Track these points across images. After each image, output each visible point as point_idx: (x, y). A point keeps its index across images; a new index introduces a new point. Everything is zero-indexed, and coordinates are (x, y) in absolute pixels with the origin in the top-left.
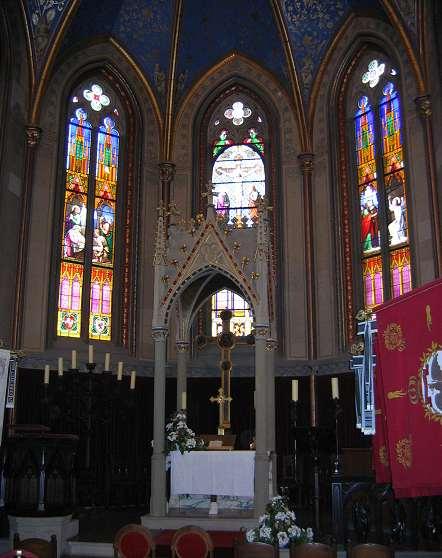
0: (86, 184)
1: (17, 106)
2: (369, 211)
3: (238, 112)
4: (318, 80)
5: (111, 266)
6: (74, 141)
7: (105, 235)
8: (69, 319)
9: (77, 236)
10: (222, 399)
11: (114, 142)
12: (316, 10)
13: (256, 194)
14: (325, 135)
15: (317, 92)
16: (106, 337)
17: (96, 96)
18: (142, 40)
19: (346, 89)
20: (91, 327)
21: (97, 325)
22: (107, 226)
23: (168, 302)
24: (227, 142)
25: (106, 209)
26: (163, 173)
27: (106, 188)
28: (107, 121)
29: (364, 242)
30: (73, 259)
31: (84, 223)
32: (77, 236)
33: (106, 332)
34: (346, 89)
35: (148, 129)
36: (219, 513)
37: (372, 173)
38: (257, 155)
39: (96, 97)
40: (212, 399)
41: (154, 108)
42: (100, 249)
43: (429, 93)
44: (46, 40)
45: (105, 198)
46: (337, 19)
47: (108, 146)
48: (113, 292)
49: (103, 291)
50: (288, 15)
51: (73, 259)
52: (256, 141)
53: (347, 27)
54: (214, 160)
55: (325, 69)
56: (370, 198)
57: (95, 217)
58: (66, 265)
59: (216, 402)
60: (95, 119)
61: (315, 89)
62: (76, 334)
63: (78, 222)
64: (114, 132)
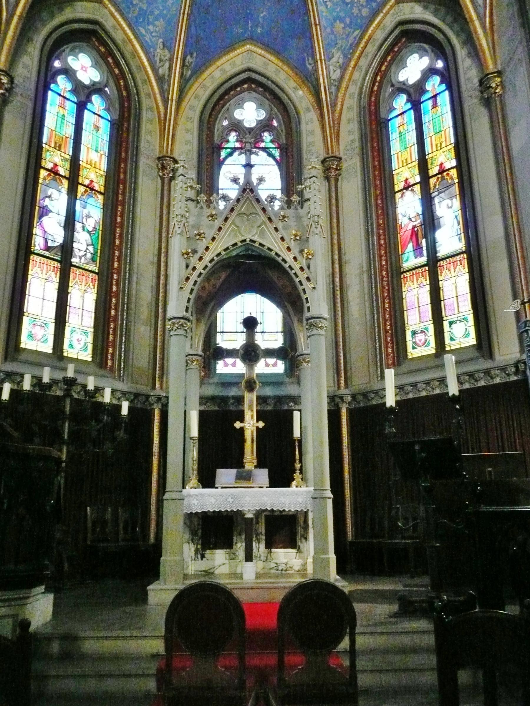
4: (347, 77)
7: (89, 232)
11: (105, 127)
14: (356, 136)
15: (346, 90)
17: (83, 67)
19: (380, 88)
24: (238, 145)
25: (91, 201)
26: (163, 168)
27: (93, 176)
28: (96, 99)
30: (47, 254)
31: (63, 213)
35: (145, 115)
38: (271, 161)
41: (154, 94)
42: (83, 247)
43: (499, 67)
49: (84, 299)
51: (47, 254)
53: (386, 15)
54: (221, 163)
58: (38, 259)
61: (344, 85)
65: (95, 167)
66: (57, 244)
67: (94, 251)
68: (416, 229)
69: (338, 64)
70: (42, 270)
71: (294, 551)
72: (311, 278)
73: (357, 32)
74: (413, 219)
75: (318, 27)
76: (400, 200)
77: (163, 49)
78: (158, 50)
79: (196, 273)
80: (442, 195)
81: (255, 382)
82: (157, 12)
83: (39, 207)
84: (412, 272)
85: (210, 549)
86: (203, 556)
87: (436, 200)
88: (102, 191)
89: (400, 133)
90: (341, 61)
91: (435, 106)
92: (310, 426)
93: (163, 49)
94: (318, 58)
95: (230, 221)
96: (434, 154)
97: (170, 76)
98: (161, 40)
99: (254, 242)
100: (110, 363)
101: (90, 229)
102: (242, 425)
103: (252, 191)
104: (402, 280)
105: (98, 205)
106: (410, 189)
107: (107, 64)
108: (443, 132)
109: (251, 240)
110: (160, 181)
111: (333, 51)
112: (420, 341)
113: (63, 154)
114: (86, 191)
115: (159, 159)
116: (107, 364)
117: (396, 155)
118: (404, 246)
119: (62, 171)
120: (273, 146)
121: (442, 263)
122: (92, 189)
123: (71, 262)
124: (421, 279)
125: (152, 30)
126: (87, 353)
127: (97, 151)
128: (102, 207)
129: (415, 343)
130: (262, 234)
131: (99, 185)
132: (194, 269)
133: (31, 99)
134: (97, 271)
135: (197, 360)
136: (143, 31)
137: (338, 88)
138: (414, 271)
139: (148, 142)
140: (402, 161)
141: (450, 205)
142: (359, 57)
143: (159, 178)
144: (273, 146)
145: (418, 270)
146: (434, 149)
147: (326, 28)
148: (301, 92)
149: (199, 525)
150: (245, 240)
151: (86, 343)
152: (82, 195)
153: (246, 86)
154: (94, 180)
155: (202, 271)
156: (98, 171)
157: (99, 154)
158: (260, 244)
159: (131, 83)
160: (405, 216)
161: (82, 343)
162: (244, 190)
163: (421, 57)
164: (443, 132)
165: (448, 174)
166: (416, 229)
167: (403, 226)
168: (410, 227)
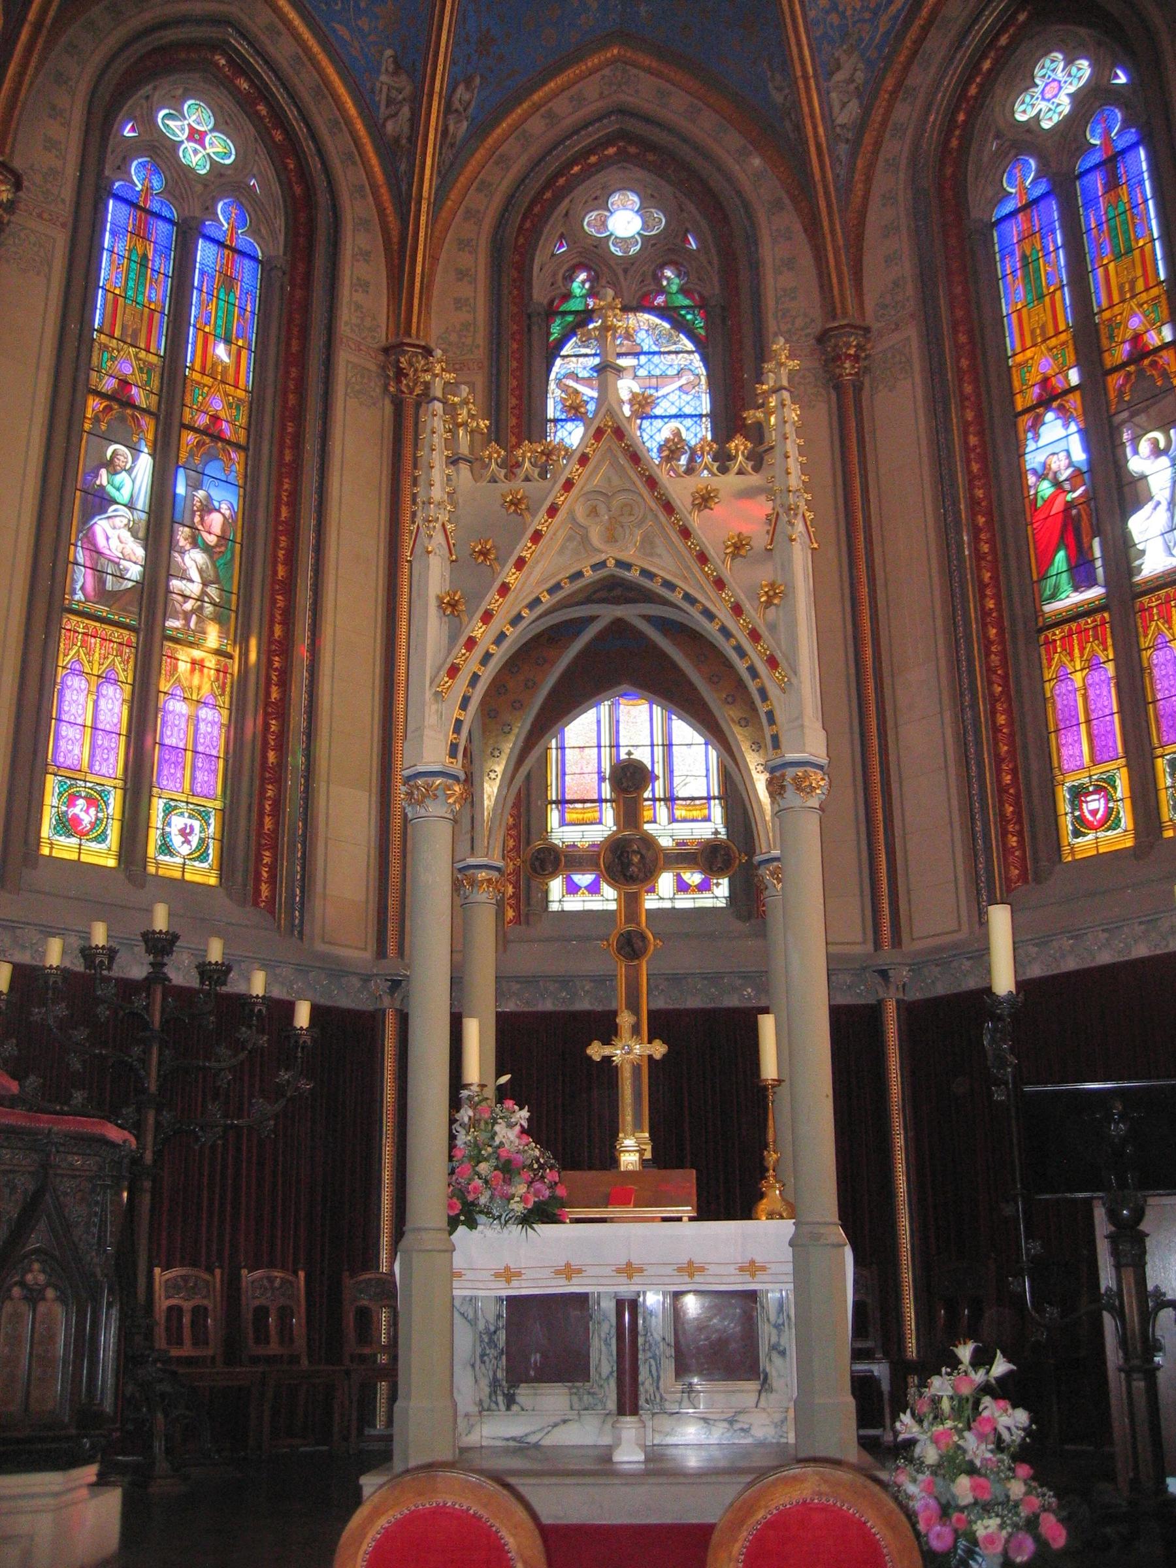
0: (155, 384)
2: (1057, 484)
3: (625, 221)
6: (120, 247)
7: (207, 549)
8: (81, 803)
9: (117, 538)
10: (631, 1051)
11: (248, 274)
14: (906, 268)
15: (876, 152)
16: (204, 873)
20: (154, 836)
21: (174, 830)
22: (216, 521)
23: (461, 684)
25: (213, 469)
27: (218, 406)
29: (1044, 577)
30: (102, 610)
31: (142, 502)
32: (117, 538)
33: (202, 857)
34: (964, 147)
36: (647, 1460)
37: (1063, 371)
39: (196, 136)
40: (596, 1051)
42: (194, 589)
47: (229, 281)
55: (899, 85)
56: (1055, 447)
57: (181, 490)
59: (607, 1059)
60: (191, 196)
61: (868, 139)
62: (103, 854)
63: (123, 496)
65: (223, 382)
66: (130, 584)
67: (220, 597)
68: (1074, 512)
69: (852, 87)
71: (753, 1386)
72: (779, 656)
74: (1067, 486)
77: (395, 73)
78: (383, 78)
79: (478, 652)
81: (643, 937)
84: (1066, 627)
86: (510, 1400)
89: (1024, 257)
90: (860, 76)
91: (1112, 185)
93: (395, 73)
94: (799, 74)
95: (561, 514)
96: (1116, 310)
97: (412, 140)
98: (389, 52)
99: (628, 566)
101: (212, 540)
103: (619, 433)
104: (1043, 650)
105: (231, 479)
106: (1055, 404)
107: (255, 117)
108: (1137, 252)
109: (620, 564)
110: (389, 408)
112: (1094, 813)
113: (143, 354)
114: (200, 445)
115: (386, 350)
116: (257, 892)
117: (1014, 316)
118: (1046, 561)
119: (139, 396)
120: (687, 302)
121: (1145, 599)
122: (218, 438)
123: (164, 628)
124: (1093, 646)
125: (366, 28)
126: (206, 865)
127: (228, 341)
128: (241, 482)
129: (1081, 820)
131: (234, 427)
132: (471, 643)
133: (64, 225)
136: (342, 31)
137: (856, 145)
138: (1074, 626)
139: (358, 307)
140: (1033, 332)
143: (387, 401)
144: (687, 302)
145: (1082, 621)
146: (1116, 299)
148: (757, 162)
149: (499, 1316)
150: (603, 564)
151: (202, 840)
152: (191, 454)
153: (611, 151)
154: (222, 415)
155: (493, 649)
158: (645, 573)
160: (1041, 477)
161: (195, 839)
164: (1137, 252)
165: (1154, 364)
166: (1074, 512)
167: (1040, 503)
168: (1058, 507)
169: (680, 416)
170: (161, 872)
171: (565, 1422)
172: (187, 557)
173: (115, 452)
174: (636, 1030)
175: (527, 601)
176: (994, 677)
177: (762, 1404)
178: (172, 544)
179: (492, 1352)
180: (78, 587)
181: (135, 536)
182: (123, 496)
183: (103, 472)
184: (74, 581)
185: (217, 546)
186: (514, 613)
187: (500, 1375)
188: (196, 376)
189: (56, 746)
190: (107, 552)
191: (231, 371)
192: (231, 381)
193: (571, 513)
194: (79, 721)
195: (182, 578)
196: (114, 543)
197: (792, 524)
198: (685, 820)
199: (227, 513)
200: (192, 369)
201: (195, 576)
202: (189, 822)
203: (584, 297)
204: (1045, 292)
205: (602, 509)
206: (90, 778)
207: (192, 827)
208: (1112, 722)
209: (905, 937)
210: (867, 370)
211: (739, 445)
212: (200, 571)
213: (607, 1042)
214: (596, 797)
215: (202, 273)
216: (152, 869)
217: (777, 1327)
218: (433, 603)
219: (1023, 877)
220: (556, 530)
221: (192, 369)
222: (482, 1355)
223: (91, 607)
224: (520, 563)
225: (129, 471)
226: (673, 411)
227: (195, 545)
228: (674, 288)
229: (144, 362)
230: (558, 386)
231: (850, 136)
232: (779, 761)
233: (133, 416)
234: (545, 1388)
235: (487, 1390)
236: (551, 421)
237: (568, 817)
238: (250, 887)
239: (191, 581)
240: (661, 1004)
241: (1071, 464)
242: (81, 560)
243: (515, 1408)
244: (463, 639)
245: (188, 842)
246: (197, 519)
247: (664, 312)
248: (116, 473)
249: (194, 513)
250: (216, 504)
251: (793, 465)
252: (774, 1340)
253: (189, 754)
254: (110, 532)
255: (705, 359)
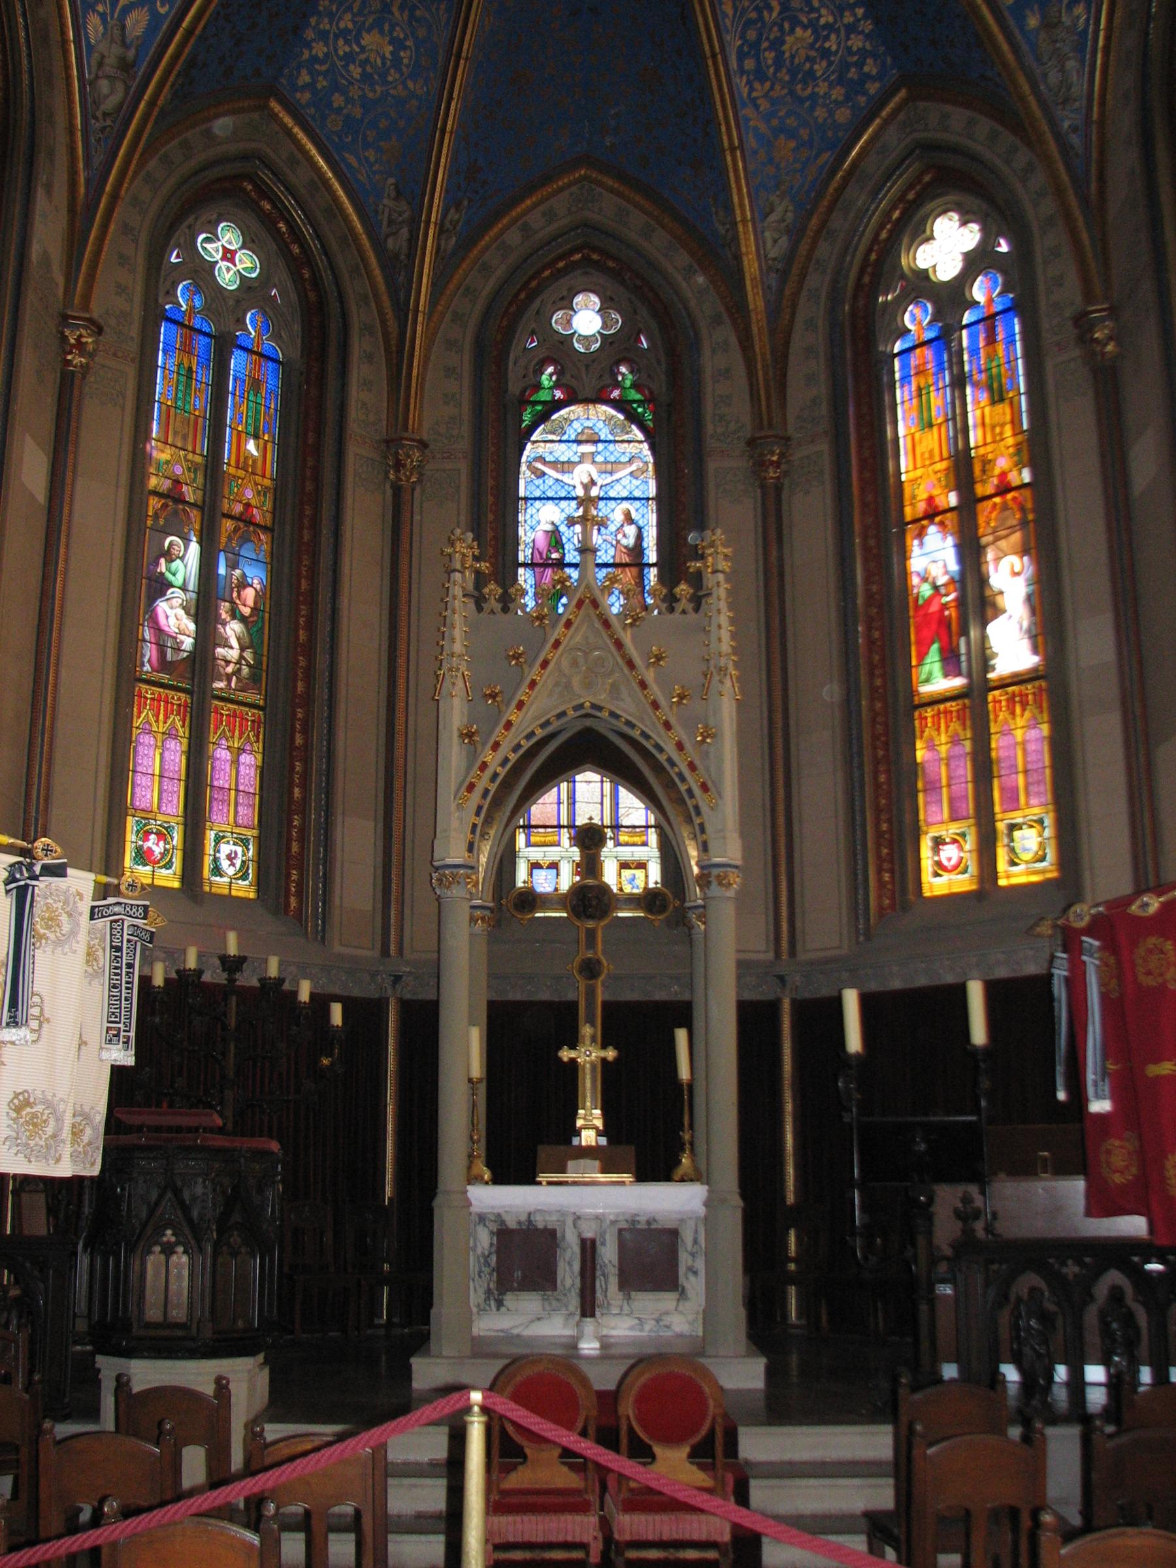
0: (200, 480)
1: (46, 259)
2: (936, 588)
3: (586, 320)
5: (258, 699)
6: (172, 363)
7: (243, 619)
8: (153, 837)
9: (174, 616)
10: (588, 1055)
11: (272, 379)
12: (811, 74)
13: (631, 530)
14: (822, 389)
16: (245, 889)
18: (358, 112)
20: (208, 861)
21: (222, 856)
22: (249, 594)
23: (476, 797)
24: (558, 394)
25: (247, 551)
27: (249, 494)
29: (921, 662)
30: (164, 677)
31: (192, 585)
32: (174, 616)
33: (244, 877)
40: (566, 1054)
42: (233, 654)
44: (120, 87)
45: (244, 519)
46: (862, 100)
47: (256, 385)
48: (264, 772)
49: (238, 766)
50: (741, 83)
51: (164, 677)
52: (634, 395)
55: (823, 224)
56: (932, 558)
57: (222, 571)
58: (149, 692)
59: (573, 1061)
61: (795, 271)
62: (169, 878)
63: (178, 580)
64: (269, 345)
65: (253, 473)
66: (185, 654)
67: (254, 660)
70: (157, 716)
71: (673, 1296)
72: (710, 784)
73: (826, 156)
74: (943, 591)
75: (738, 153)
76: (916, 542)
77: (397, 199)
78: (385, 201)
79: (488, 773)
80: (1003, 544)
81: (599, 962)
82: (383, 123)
83: (149, 579)
84: (936, 707)
85: (512, 1290)
86: (500, 1304)
87: (990, 555)
88: (269, 524)
92: (707, 1062)
97: (411, 255)
98: (391, 180)
99: (600, 708)
100: (293, 902)
101: (246, 611)
102: (573, 1054)
103: (595, 604)
105: (261, 557)
106: (937, 519)
109: (593, 706)
110: (389, 492)
111: (772, 198)
112: (949, 859)
113: (190, 456)
114: (236, 529)
116: (288, 904)
119: (189, 493)
120: (638, 397)
122: (250, 522)
125: (372, 159)
126: (247, 882)
127: (256, 437)
128: (268, 560)
129: (939, 864)
130: (614, 690)
133: (133, 360)
134: (261, 703)
135: (483, 919)
136: (352, 160)
139: (364, 404)
140: (922, 454)
141: (1017, 569)
142: (830, 209)
143: (388, 486)
144: (638, 397)
145: (948, 704)
147: (755, 152)
148: (701, 279)
149: (491, 1244)
150: (581, 706)
152: (230, 538)
153: (578, 256)
154: (253, 502)
155: (499, 769)
156: (258, 479)
157: (261, 441)
159: (327, 277)
160: (924, 579)
161: (238, 863)
162: (580, 604)
163: (964, 223)
167: (921, 602)
168: (934, 608)
169: (631, 499)
170: (213, 890)
171: (539, 1319)
172: (227, 628)
173: (171, 544)
174: (593, 1039)
175: (525, 733)
176: (878, 743)
177: (681, 1308)
178: (218, 619)
179: (486, 1270)
180: (146, 660)
181: (188, 613)
182: (178, 580)
183: (162, 561)
184: (143, 656)
185: (251, 616)
186: (516, 742)
187: (492, 1286)
188: (232, 471)
189: (133, 794)
190: (167, 629)
191: (260, 463)
192: (259, 471)
193: (558, 663)
194: (150, 771)
195: (225, 646)
196: (172, 621)
197: (721, 682)
198: (627, 844)
199: (258, 587)
200: (229, 464)
201: (234, 642)
202: (234, 848)
203: (551, 388)
204: (934, 422)
205: (581, 661)
206: (159, 817)
207: (236, 853)
208: (967, 789)
209: (799, 947)
210: (786, 474)
211: (683, 589)
212: (238, 639)
213: (573, 1047)
214: (555, 823)
215: (235, 380)
216: (207, 889)
217: (693, 1255)
218: (456, 734)
219: (893, 907)
220: (546, 679)
221: (229, 464)
222: (480, 1272)
223: (156, 676)
224: (520, 705)
225: (182, 558)
226: (625, 494)
227: (234, 617)
228: (628, 383)
229: (192, 462)
230: (528, 467)
231: (779, 266)
232: (707, 863)
233: (184, 510)
234: (524, 1295)
235: (483, 1296)
236: (522, 499)
237: (533, 839)
238: (282, 900)
239: (231, 648)
240: (608, 997)
241: (946, 572)
242: (147, 637)
243: (503, 1309)
244: (478, 764)
245: (233, 865)
246: (235, 594)
247: (620, 405)
248: (173, 561)
249: (232, 589)
250: (249, 580)
251: (725, 635)
252: (690, 1263)
253: (233, 792)
254: (169, 612)
255: (653, 448)
